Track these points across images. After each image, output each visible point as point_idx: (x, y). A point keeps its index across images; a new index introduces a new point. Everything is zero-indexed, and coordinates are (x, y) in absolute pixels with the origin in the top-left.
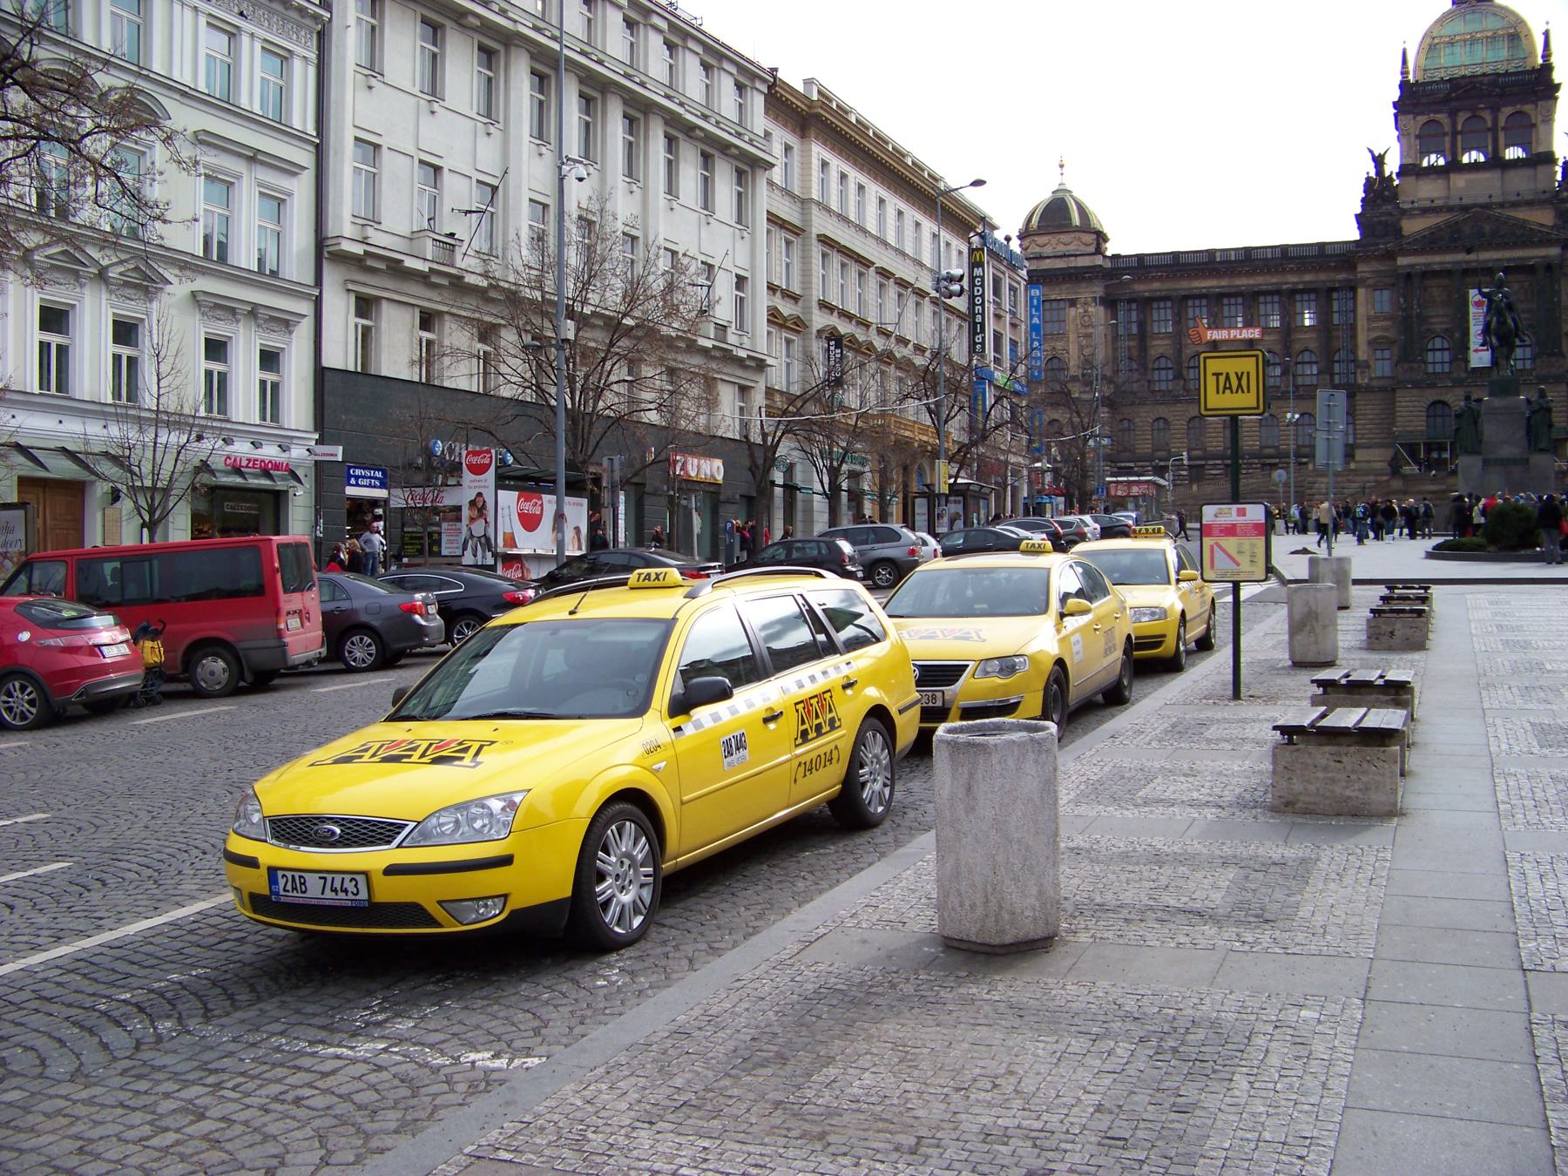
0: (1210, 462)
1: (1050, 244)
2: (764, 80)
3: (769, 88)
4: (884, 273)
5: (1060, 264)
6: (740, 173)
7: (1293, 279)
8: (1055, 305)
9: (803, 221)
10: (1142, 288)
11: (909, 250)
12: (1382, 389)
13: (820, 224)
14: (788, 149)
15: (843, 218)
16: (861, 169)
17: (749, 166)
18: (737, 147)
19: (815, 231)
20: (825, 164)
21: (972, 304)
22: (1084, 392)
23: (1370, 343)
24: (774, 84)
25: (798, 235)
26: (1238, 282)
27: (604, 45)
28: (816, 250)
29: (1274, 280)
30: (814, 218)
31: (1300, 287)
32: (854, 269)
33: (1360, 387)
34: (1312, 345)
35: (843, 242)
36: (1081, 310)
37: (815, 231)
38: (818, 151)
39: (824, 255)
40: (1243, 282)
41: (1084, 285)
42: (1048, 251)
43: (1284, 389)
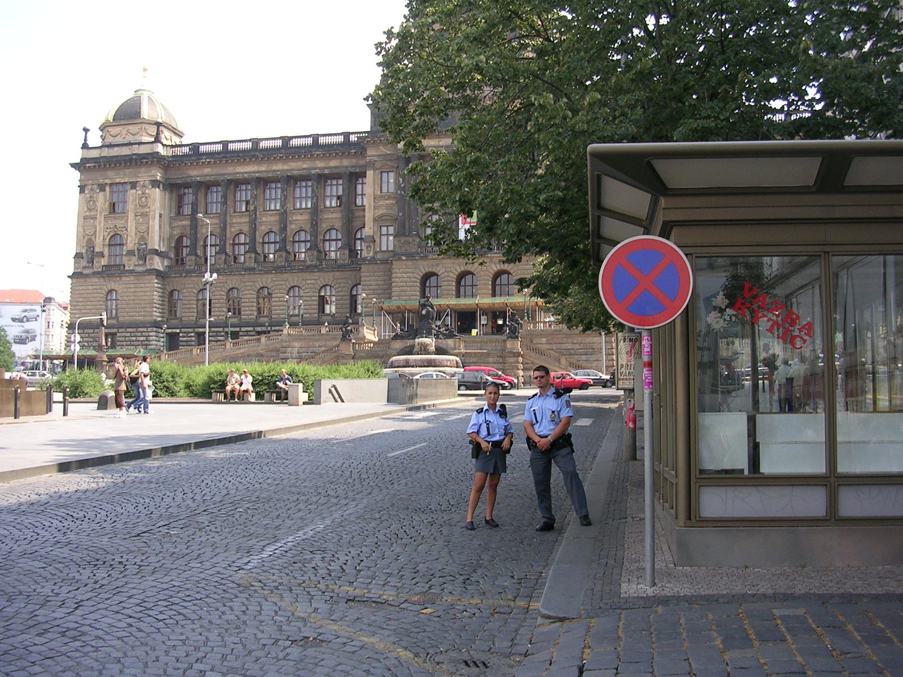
0: (243, 329)
1: (122, 134)
5: (125, 151)
7: (320, 164)
8: (121, 188)
10: (197, 173)
12: (385, 262)
22: (139, 265)
23: (375, 220)
26: (275, 168)
29: (305, 166)
31: (326, 172)
33: (364, 259)
34: (338, 225)
36: (140, 192)
40: (280, 167)
41: (143, 169)
42: (119, 140)
43: (309, 263)
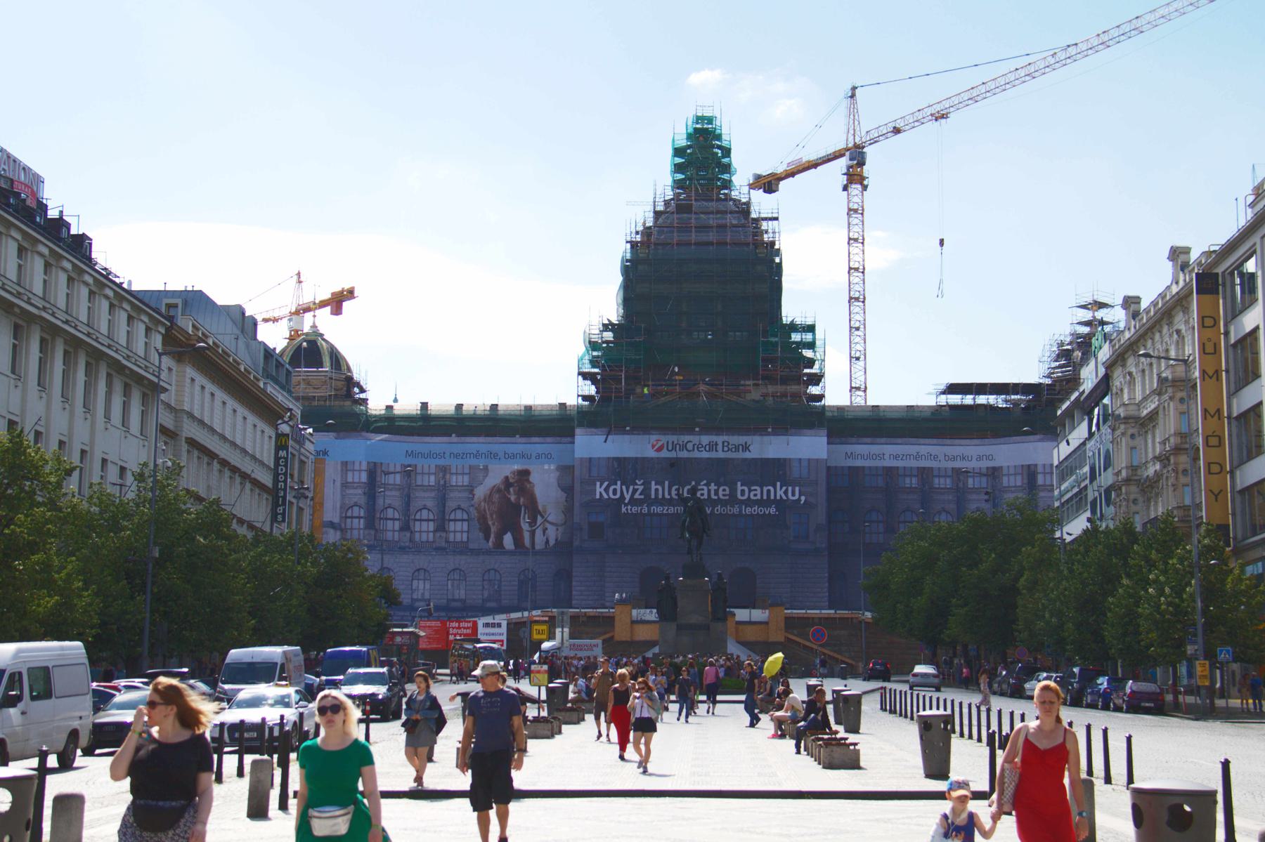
2: (164, 324)
3: (168, 329)
4: (224, 463)
6: (144, 395)
9: (176, 427)
11: (238, 442)
13: (190, 430)
14: (170, 369)
15: (201, 422)
16: (213, 382)
17: (152, 390)
18: (147, 379)
19: (184, 435)
20: (193, 380)
21: (276, 481)
24: (172, 327)
25: (172, 438)
27: (118, 339)
28: (185, 447)
30: (185, 425)
32: (206, 459)
35: (202, 442)
37: (184, 435)
38: (190, 372)
39: (189, 452)
